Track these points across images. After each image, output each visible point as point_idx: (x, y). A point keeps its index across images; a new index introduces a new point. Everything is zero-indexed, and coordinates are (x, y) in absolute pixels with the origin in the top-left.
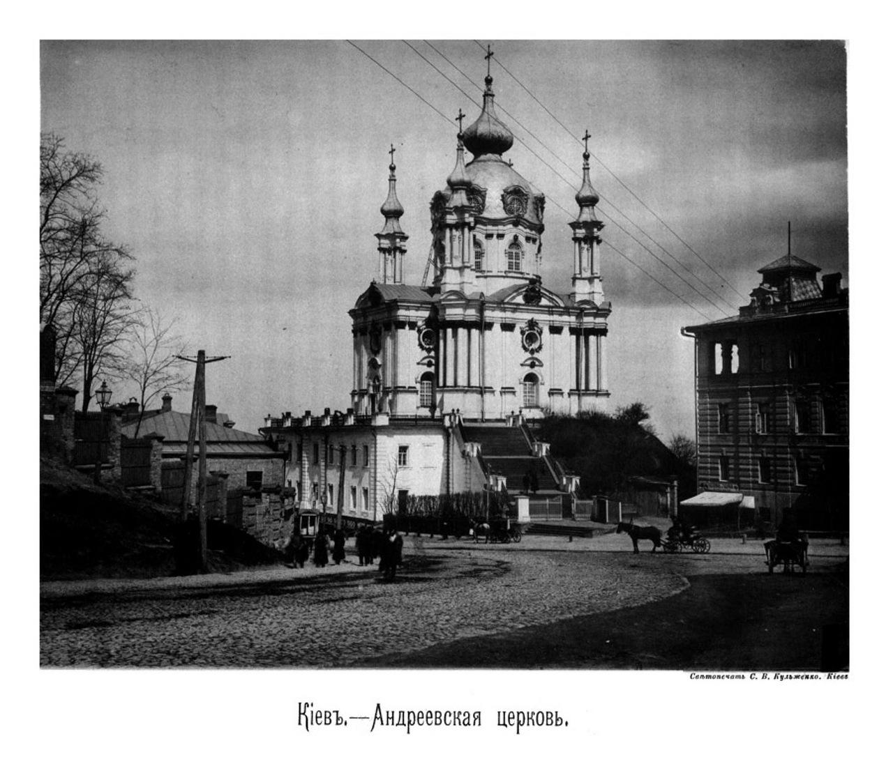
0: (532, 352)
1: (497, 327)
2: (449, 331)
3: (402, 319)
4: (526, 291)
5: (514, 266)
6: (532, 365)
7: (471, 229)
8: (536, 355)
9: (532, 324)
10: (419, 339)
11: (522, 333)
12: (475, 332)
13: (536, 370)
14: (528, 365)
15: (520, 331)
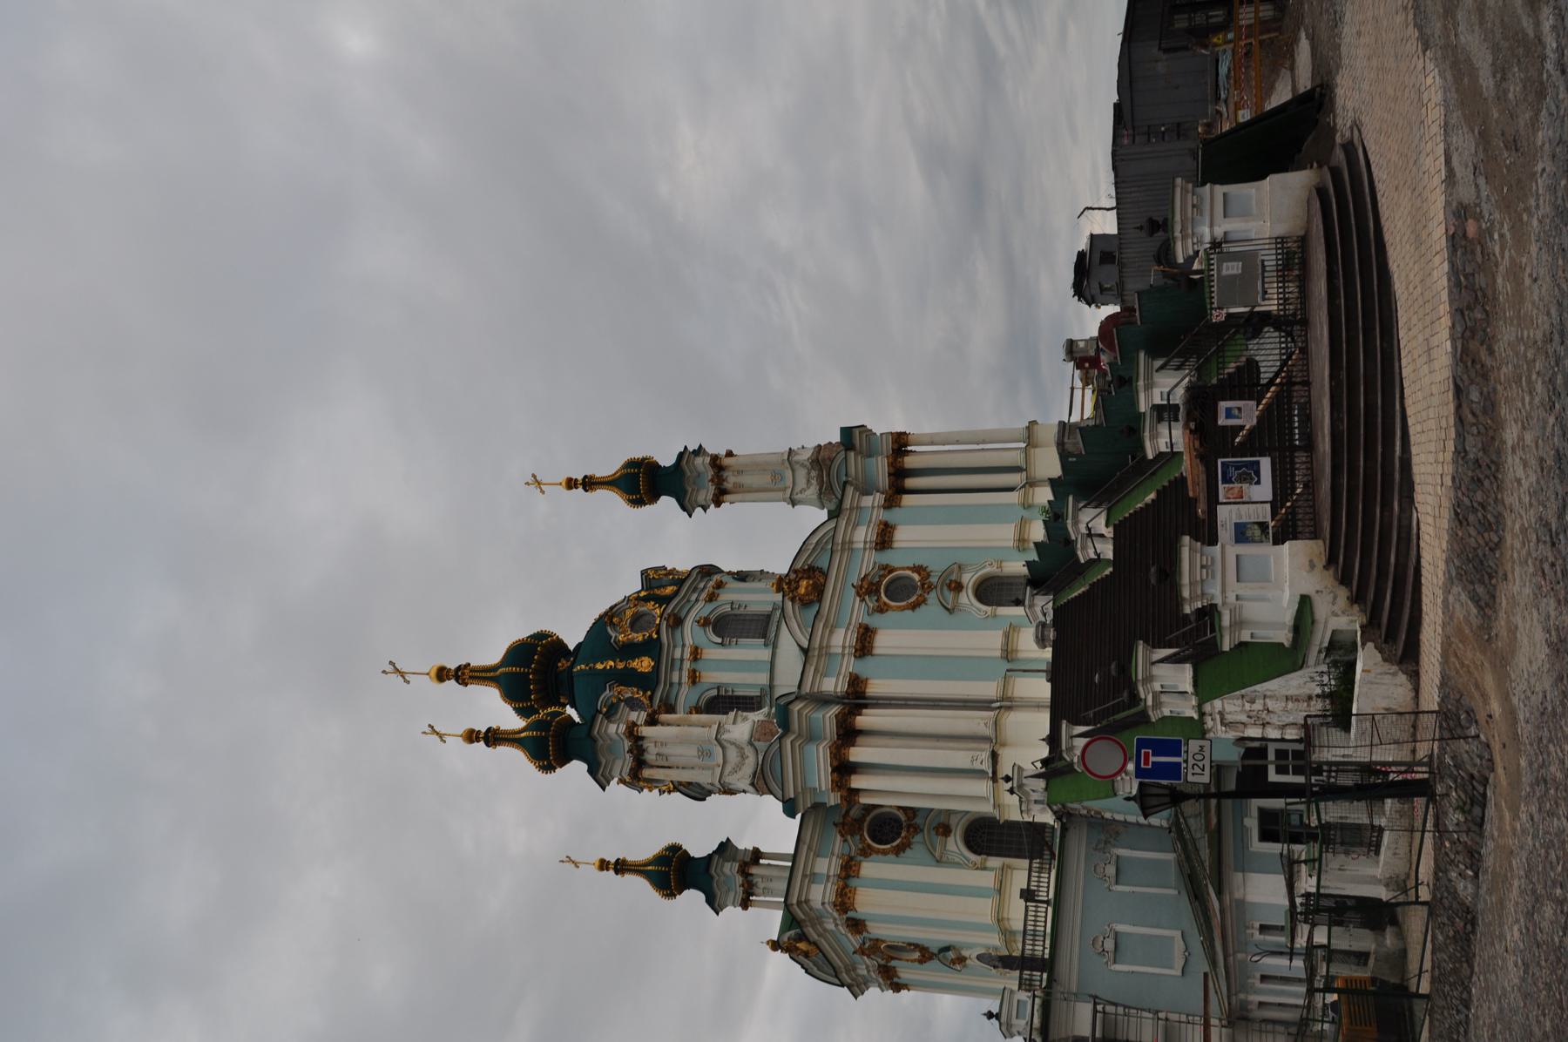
0: (927, 587)
1: (864, 668)
2: (857, 782)
3: (831, 896)
4: (793, 600)
5: (761, 627)
6: (958, 587)
7: (652, 721)
8: (934, 580)
9: (867, 589)
10: (884, 853)
11: (881, 610)
12: (868, 719)
13: (969, 579)
14: (956, 599)
15: (877, 615)
